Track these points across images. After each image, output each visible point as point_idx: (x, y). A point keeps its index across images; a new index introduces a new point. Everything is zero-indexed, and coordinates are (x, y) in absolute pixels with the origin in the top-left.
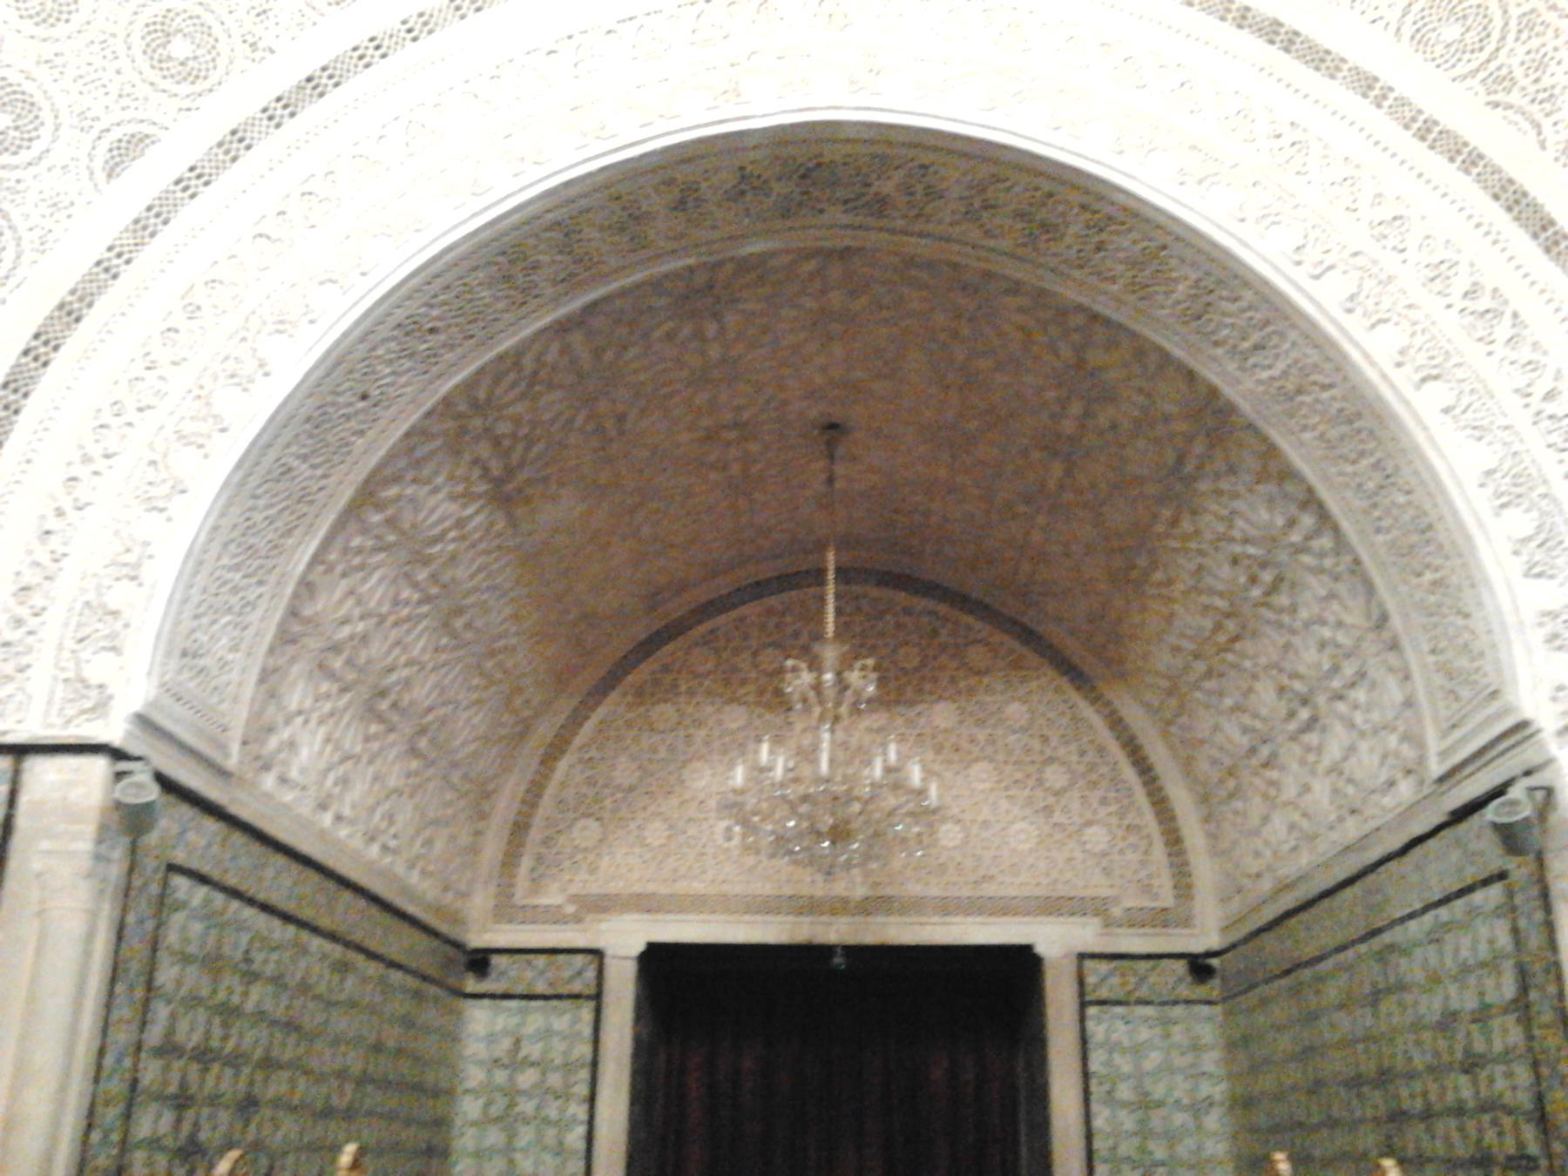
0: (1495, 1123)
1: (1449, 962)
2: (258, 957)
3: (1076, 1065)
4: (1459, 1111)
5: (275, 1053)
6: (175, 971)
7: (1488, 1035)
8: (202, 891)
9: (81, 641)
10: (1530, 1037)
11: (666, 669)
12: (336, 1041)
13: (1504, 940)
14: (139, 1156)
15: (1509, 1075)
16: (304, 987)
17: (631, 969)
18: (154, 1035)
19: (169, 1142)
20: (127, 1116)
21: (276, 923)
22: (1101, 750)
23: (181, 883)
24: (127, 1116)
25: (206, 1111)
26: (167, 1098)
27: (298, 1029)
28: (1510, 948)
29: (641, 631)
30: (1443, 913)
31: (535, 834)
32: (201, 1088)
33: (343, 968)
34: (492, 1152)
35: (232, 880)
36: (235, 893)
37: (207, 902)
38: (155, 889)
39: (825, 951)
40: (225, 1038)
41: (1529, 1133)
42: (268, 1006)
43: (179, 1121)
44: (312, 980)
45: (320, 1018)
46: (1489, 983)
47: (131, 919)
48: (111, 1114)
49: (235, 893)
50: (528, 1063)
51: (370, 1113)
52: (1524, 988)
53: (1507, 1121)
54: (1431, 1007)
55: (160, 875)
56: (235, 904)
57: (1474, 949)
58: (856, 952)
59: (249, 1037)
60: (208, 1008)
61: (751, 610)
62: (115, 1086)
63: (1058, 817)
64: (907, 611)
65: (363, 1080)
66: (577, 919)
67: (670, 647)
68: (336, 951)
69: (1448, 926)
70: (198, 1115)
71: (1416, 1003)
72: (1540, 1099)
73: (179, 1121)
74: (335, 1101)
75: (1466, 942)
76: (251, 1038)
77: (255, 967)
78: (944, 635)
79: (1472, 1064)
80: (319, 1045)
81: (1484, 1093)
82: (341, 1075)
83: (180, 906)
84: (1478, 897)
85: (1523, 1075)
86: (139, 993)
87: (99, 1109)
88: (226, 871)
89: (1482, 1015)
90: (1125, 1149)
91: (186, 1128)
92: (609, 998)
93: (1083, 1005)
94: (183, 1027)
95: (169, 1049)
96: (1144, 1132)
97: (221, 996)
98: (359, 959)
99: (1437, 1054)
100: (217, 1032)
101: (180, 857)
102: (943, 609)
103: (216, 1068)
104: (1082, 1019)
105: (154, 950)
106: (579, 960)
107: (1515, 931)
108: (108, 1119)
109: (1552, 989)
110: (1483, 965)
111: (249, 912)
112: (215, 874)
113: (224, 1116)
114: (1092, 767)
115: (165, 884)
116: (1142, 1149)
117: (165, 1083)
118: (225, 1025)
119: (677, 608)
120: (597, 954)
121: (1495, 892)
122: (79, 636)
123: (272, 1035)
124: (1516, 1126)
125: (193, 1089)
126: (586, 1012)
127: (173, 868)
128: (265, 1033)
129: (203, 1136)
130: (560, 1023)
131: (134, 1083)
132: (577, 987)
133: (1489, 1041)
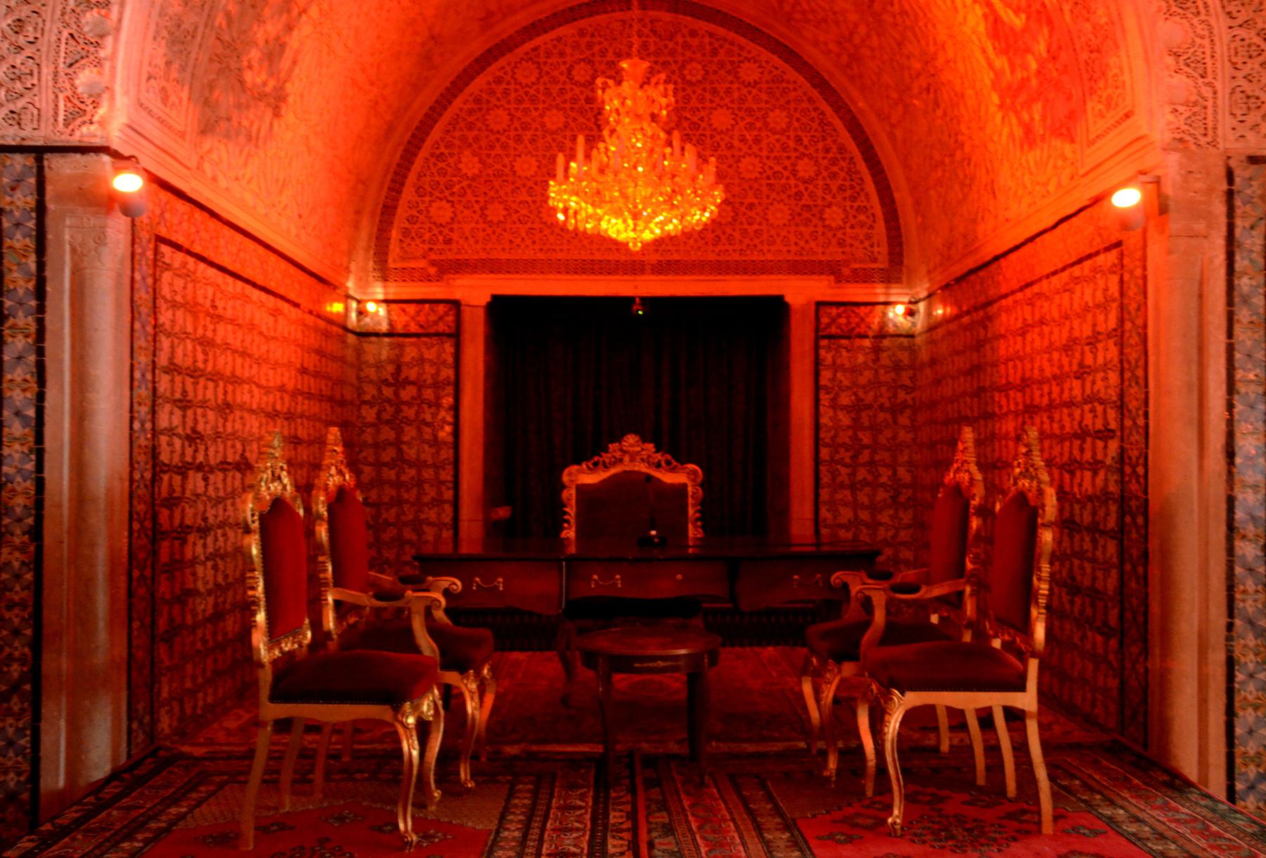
0: (1093, 410)
1: (1076, 306)
2: (220, 304)
3: (809, 380)
4: (1070, 404)
5: (238, 373)
6: (169, 314)
7: (1094, 352)
8: (180, 256)
9: (71, 65)
10: (1121, 353)
11: (498, 81)
12: (276, 365)
13: (1114, 289)
14: (163, 439)
15: (1105, 379)
16: (252, 327)
17: (481, 314)
18: (163, 360)
19: (180, 430)
20: (154, 412)
21: (229, 279)
22: (842, 149)
23: (164, 249)
24: (154, 412)
25: (199, 411)
26: (175, 401)
27: (250, 356)
28: (1117, 295)
29: (477, 47)
30: (1076, 271)
31: (402, 212)
32: (196, 396)
33: (275, 313)
34: (388, 443)
35: (197, 249)
36: (200, 258)
37: (184, 264)
38: (150, 254)
39: (629, 300)
40: (206, 361)
41: (1112, 414)
42: (230, 340)
43: (184, 416)
44: (256, 322)
45: (264, 348)
46: (1101, 318)
47: (138, 276)
48: (143, 411)
49: (200, 258)
50: (407, 382)
51: (301, 416)
52: (1121, 321)
53: (1099, 408)
54: (1060, 336)
55: (152, 246)
56: (202, 266)
57: (1094, 296)
58: (648, 302)
59: (221, 360)
60: (193, 340)
61: (567, 31)
62: (143, 392)
63: (806, 200)
64: (693, 33)
65: (295, 394)
66: (439, 278)
67: (502, 62)
68: (271, 301)
69: (1076, 280)
70: (195, 414)
71: (1051, 333)
72: (1121, 396)
73: (184, 416)
74: (278, 407)
75: (1088, 292)
76: (225, 362)
77: (220, 311)
78: (722, 56)
79: (1082, 372)
80: (264, 368)
81: (1088, 391)
82: (282, 389)
83: (168, 267)
84: (1100, 259)
85: (1113, 377)
86: (150, 329)
87: (136, 407)
88: (193, 242)
89: (1093, 342)
90: (844, 437)
91: (190, 423)
92: (466, 336)
93: (818, 338)
94: (179, 351)
95: (173, 369)
96: (856, 425)
97: (200, 332)
98: (286, 307)
99: (1061, 367)
100: (200, 357)
101: (163, 232)
102: (721, 31)
103: (202, 381)
104: (817, 347)
105: (155, 299)
106: (441, 308)
107: (1122, 281)
108: (143, 414)
109: (1139, 322)
110: (1098, 306)
111: (212, 272)
112: (186, 245)
113: (211, 415)
114: (834, 162)
115: (156, 251)
116: (855, 438)
117: (173, 393)
118: (205, 353)
119: (507, 27)
120: (456, 305)
121: (1112, 257)
122: (69, 61)
123: (234, 360)
124: (1105, 411)
125: (191, 395)
126: (449, 348)
127: (160, 240)
128: (230, 359)
129: (200, 427)
130: (430, 354)
131: (154, 390)
132: (441, 327)
133: (1095, 358)
